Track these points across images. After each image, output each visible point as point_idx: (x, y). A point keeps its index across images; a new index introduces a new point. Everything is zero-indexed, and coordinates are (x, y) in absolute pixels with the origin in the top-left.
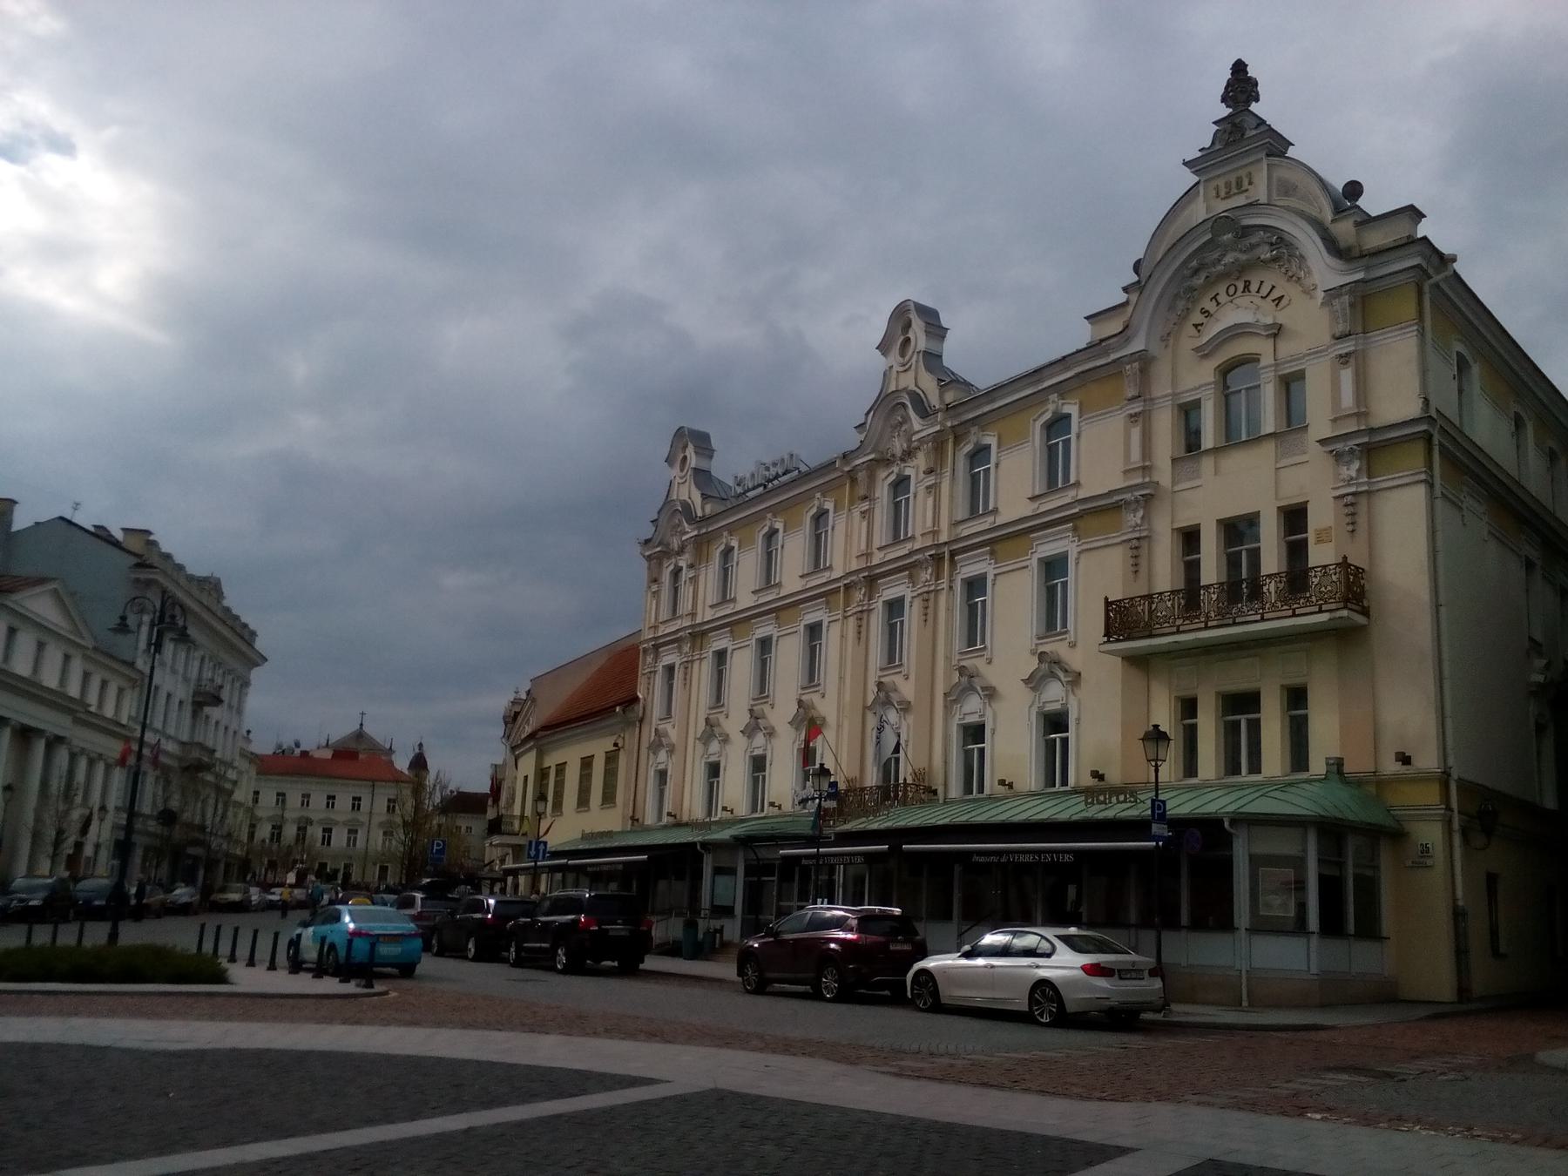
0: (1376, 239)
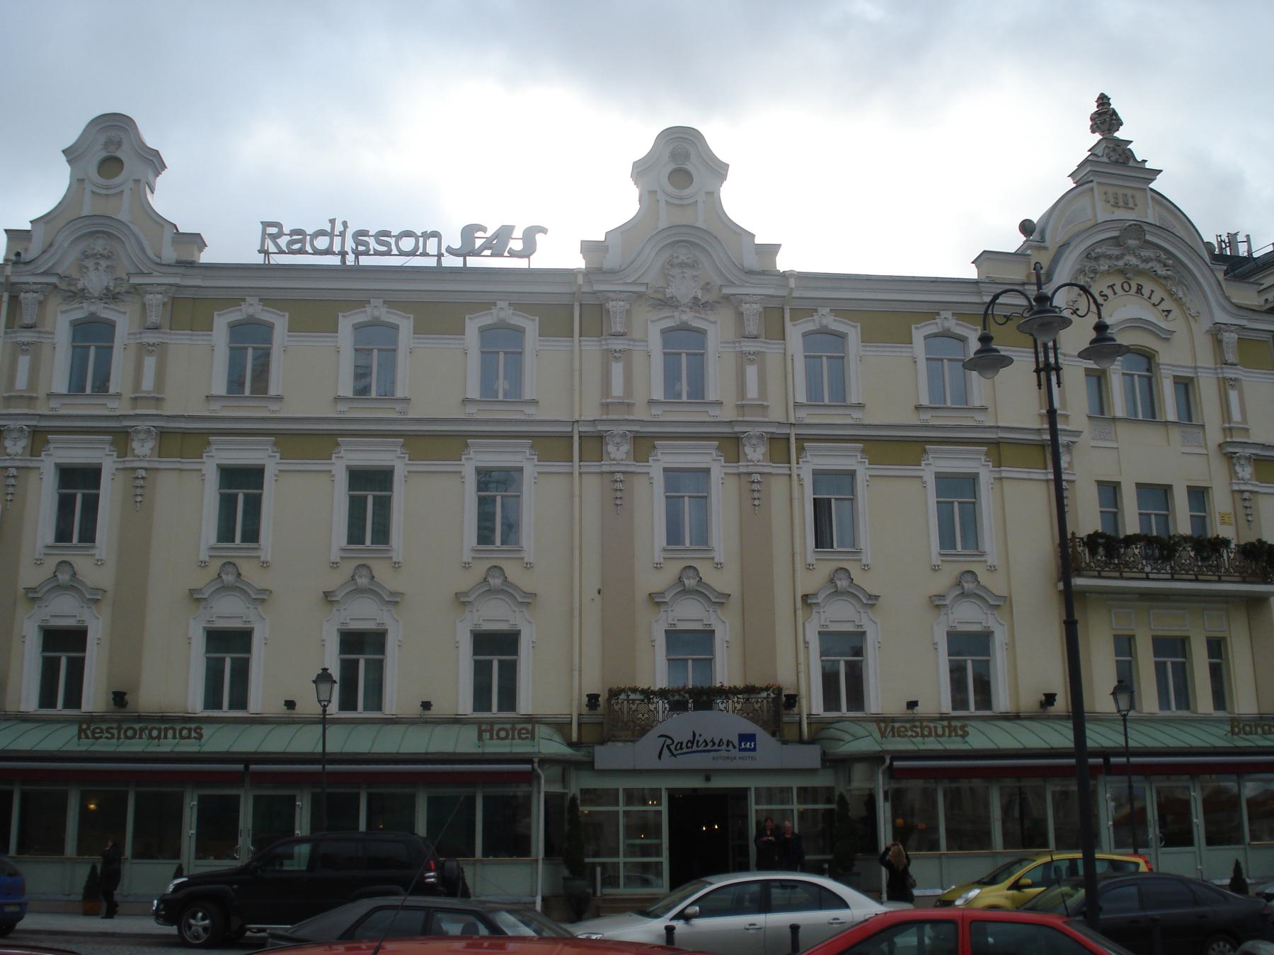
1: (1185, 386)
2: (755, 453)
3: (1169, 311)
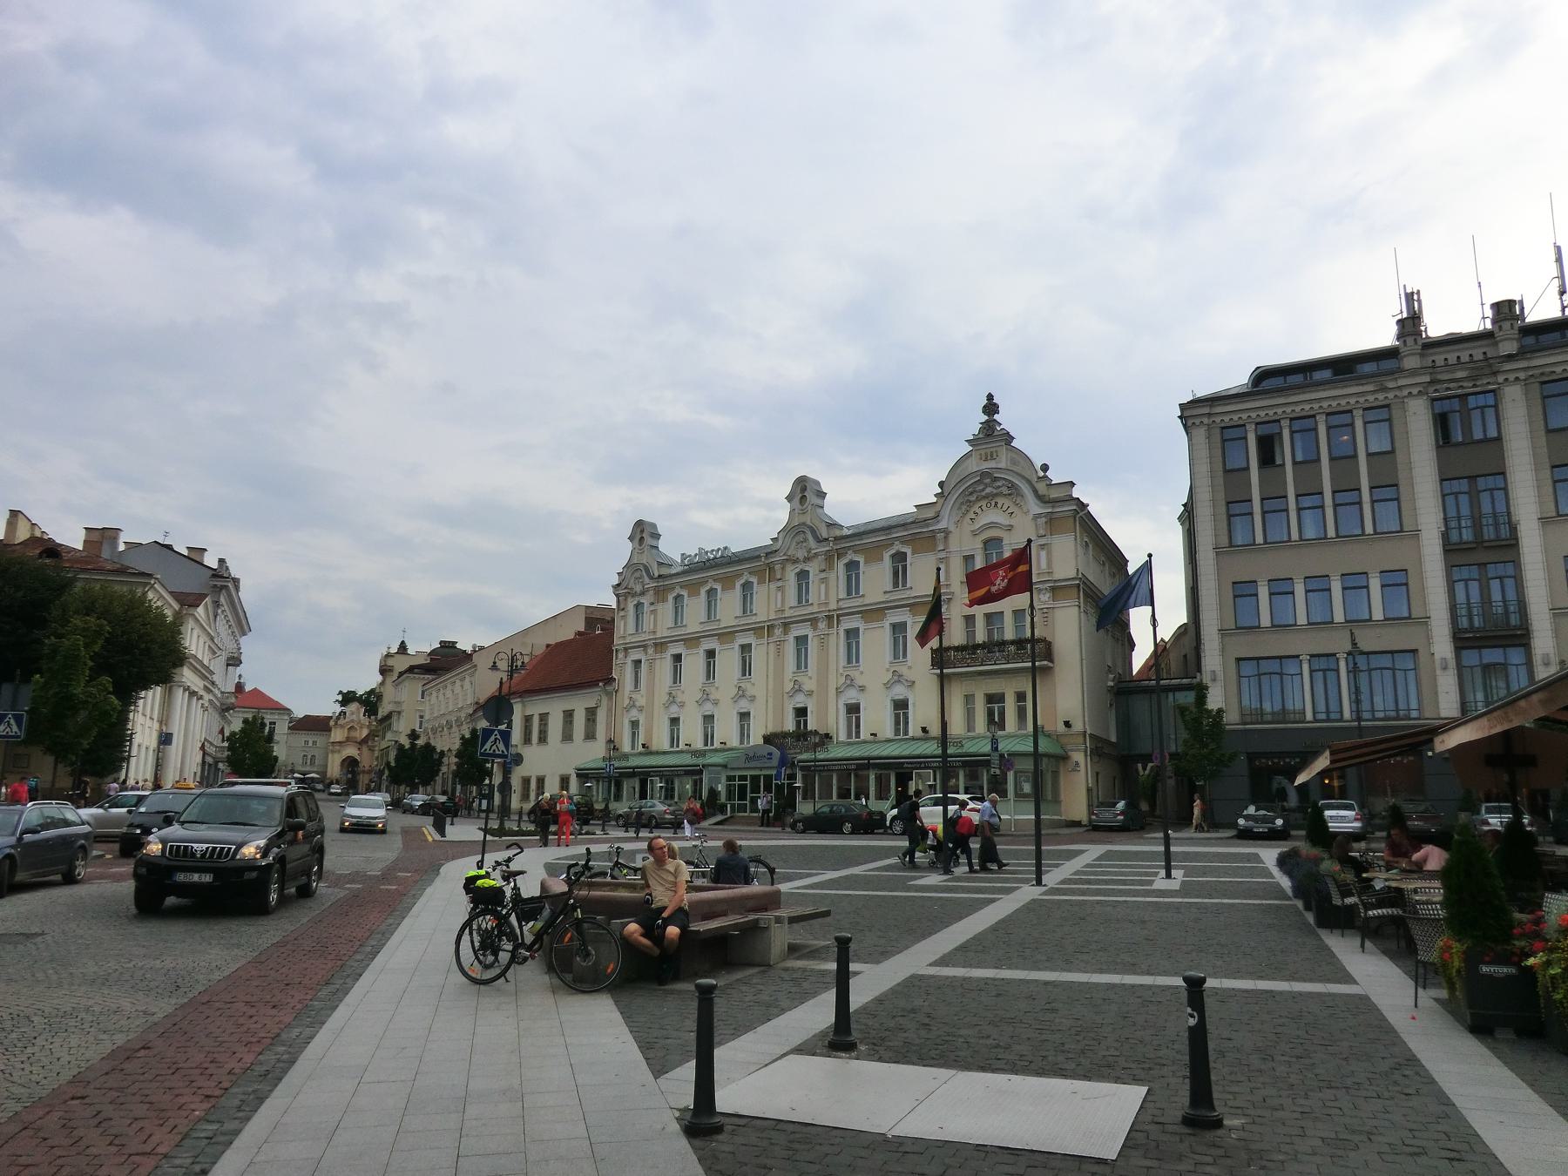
0: (1054, 494)
2: (822, 625)
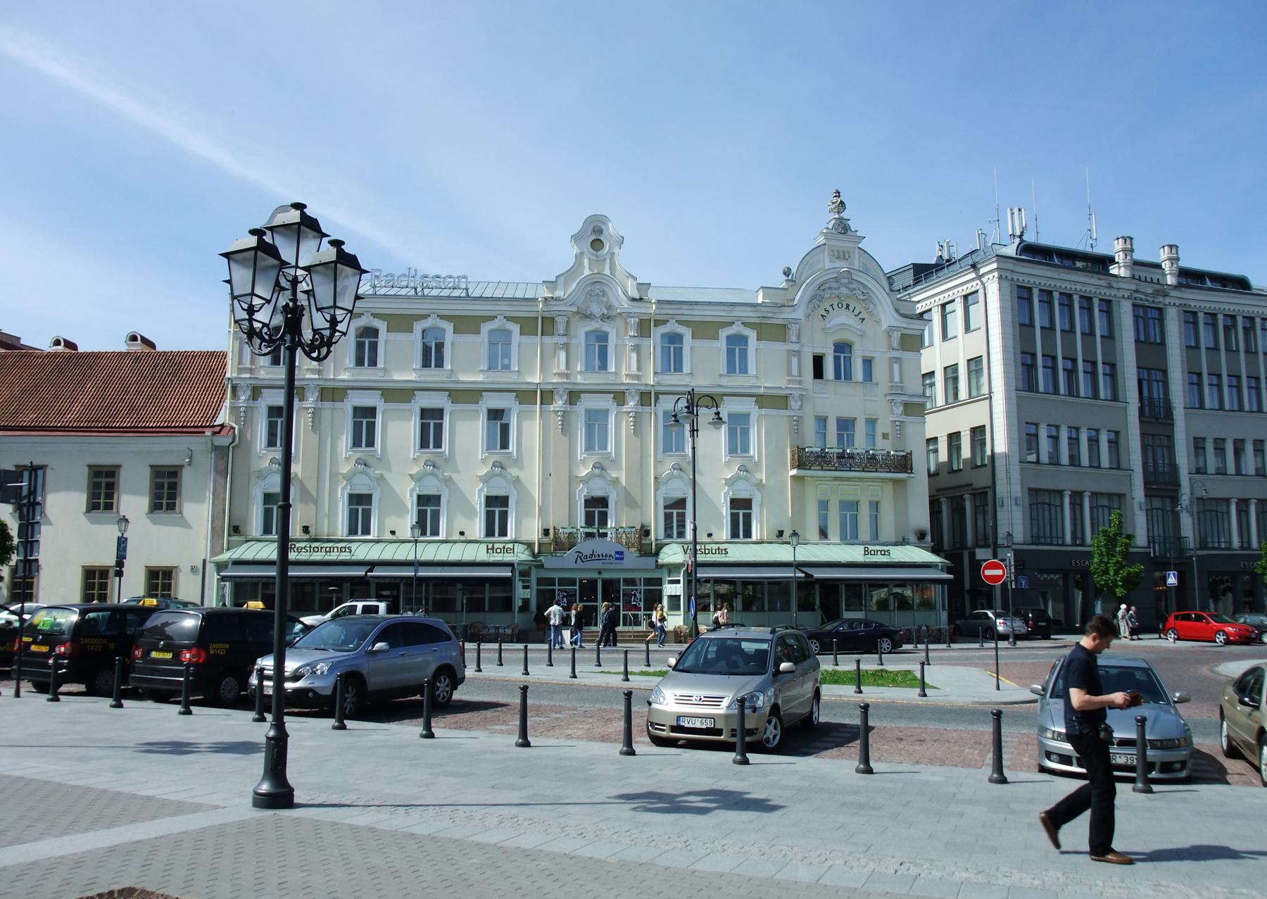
1: (868, 363)
3: (863, 319)
